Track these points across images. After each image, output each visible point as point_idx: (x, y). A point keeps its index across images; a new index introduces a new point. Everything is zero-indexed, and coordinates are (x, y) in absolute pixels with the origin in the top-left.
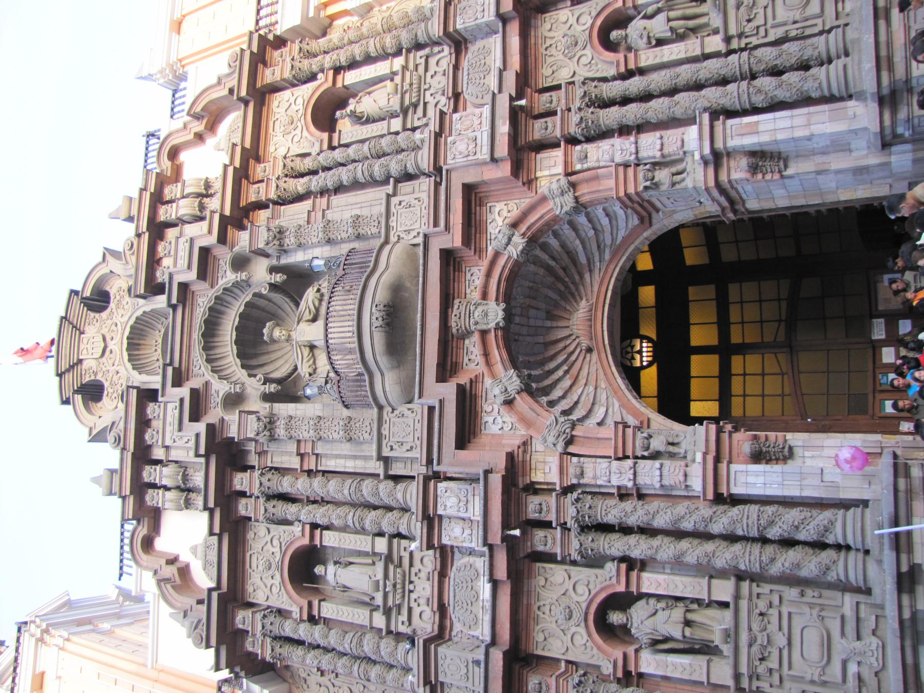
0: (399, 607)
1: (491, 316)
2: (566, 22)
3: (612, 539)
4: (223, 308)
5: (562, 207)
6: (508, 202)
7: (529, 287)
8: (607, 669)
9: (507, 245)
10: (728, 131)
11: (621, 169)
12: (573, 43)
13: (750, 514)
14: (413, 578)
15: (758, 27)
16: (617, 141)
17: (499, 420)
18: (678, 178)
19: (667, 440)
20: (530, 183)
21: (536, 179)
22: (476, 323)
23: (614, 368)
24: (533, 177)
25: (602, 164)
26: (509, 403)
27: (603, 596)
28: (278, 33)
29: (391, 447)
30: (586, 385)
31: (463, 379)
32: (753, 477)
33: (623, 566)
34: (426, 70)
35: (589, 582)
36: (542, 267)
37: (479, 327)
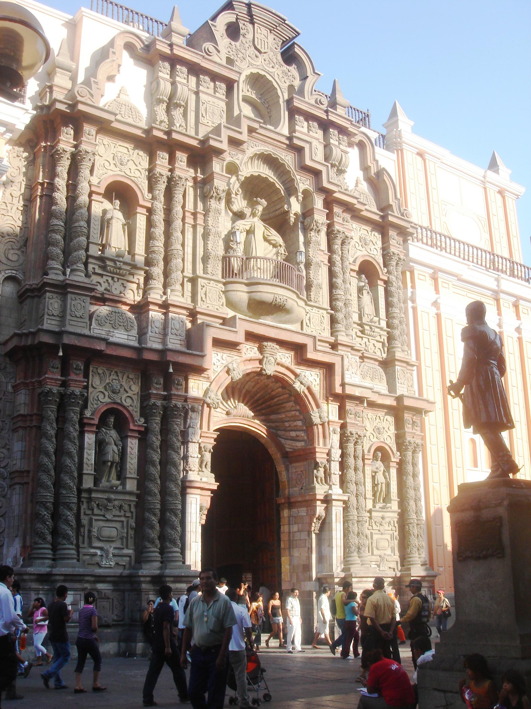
0: (104, 268)
2: (388, 429)
8: (88, 413)
14: (121, 281)
15: (372, 526)
16: (340, 451)
17: (219, 364)
18: (319, 480)
25: (331, 441)
27: (128, 415)
28: (409, 242)
29: (204, 287)
33: (143, 429)
34: (377, 341)
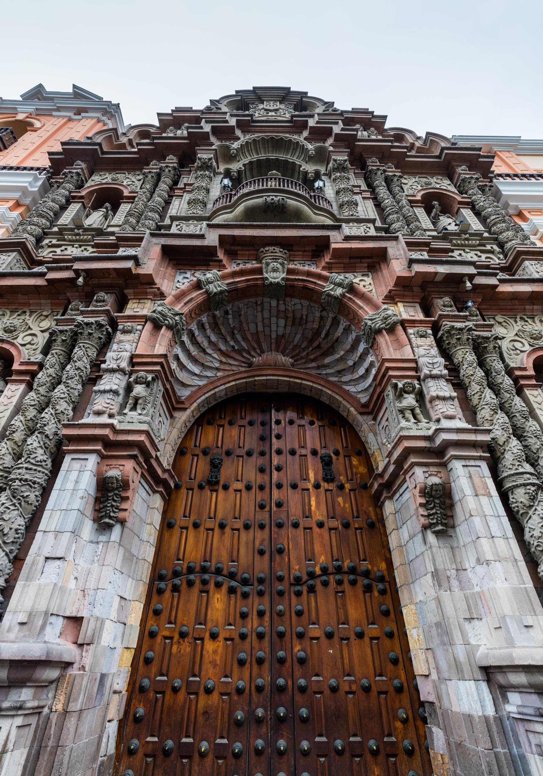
0: (64, 240)
1: (275, 275)
3: (61, 357)
4: (291, 151)
5: (371, 320)
6: (373, 286)
7: (302, 315)
9: (334, 284)
10: (472, 463)
11: (413, 365)
12: (535, 336)
13: (32, 472)
14: (83, 248)
17: (186, 281)
18: (411, 417)
19: (140, 398)
20: (391, 298)
21: (396, 304)
22: (268, 264)
23: (233, 383)
24: (397, 300)
26: (198, 285)
30: (221, 362)
31: (221, 255)
32: (75, 478)
33: (35, 368)
35: (33, 344)
36: (319, 327)
37: (264, 266)
